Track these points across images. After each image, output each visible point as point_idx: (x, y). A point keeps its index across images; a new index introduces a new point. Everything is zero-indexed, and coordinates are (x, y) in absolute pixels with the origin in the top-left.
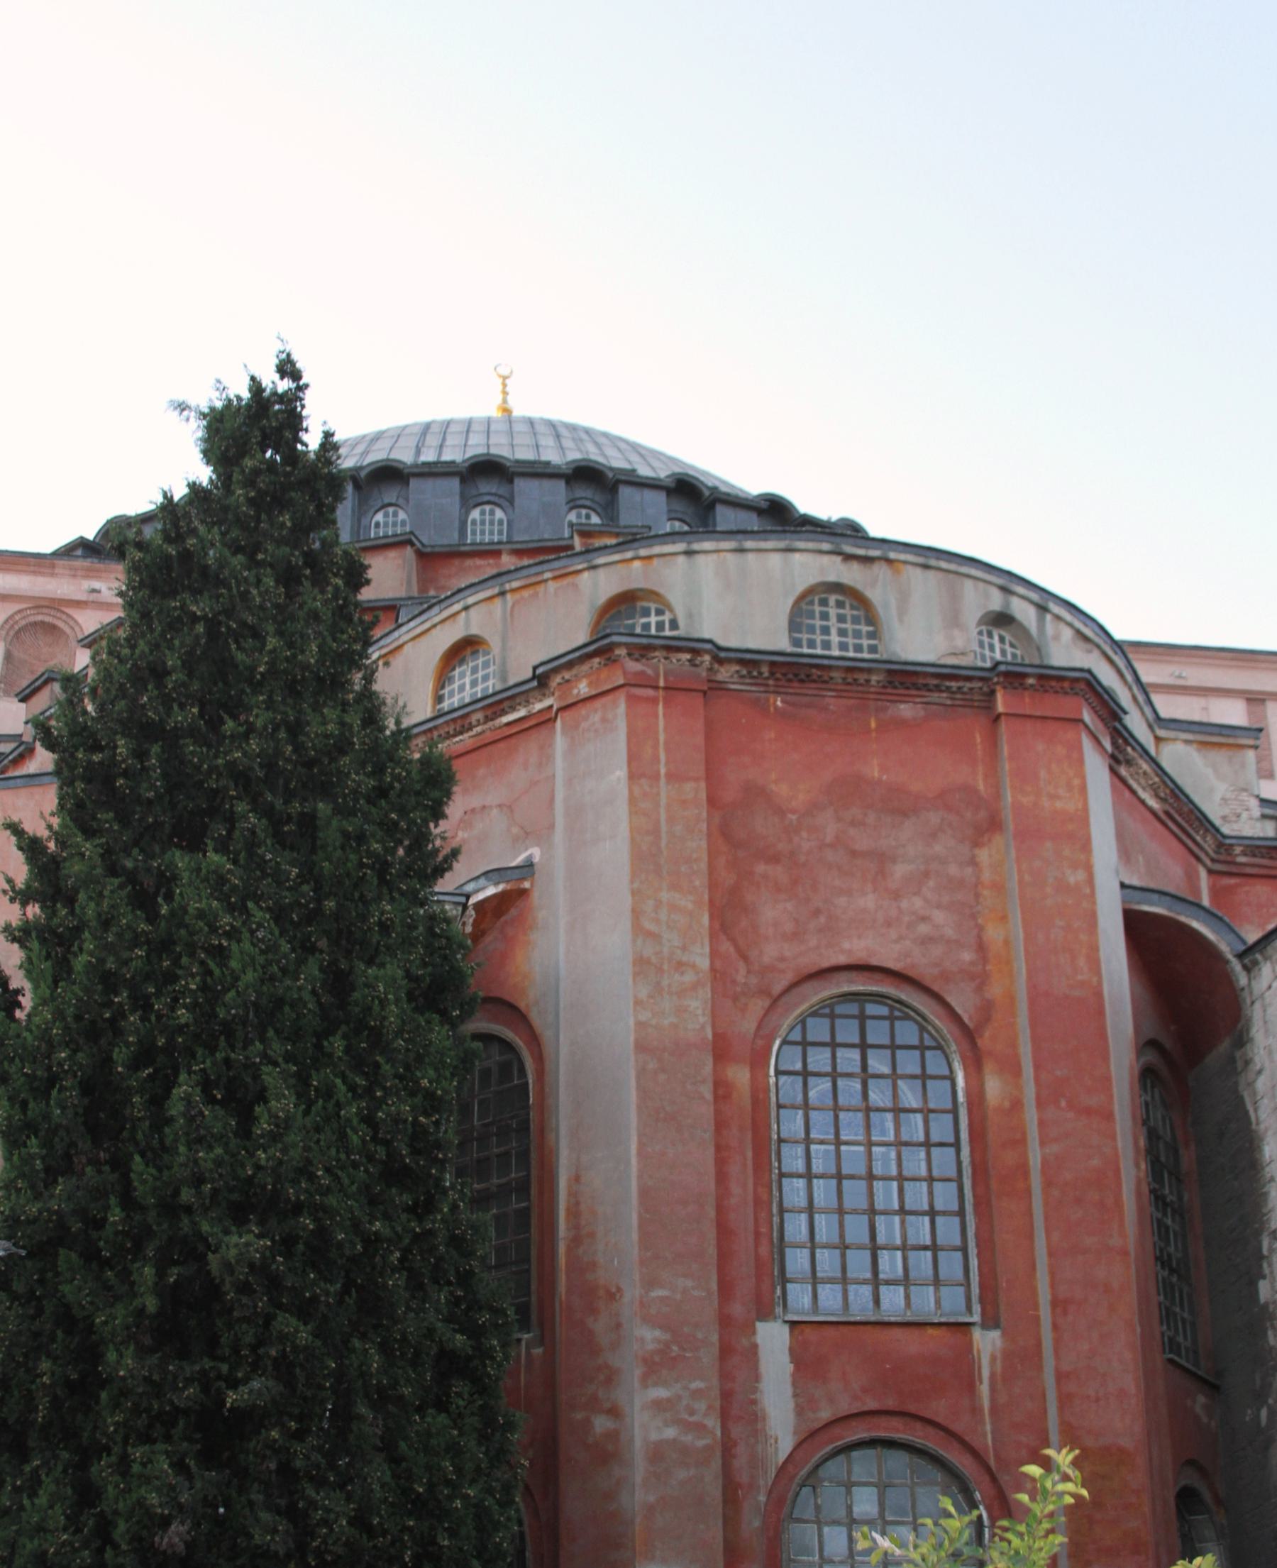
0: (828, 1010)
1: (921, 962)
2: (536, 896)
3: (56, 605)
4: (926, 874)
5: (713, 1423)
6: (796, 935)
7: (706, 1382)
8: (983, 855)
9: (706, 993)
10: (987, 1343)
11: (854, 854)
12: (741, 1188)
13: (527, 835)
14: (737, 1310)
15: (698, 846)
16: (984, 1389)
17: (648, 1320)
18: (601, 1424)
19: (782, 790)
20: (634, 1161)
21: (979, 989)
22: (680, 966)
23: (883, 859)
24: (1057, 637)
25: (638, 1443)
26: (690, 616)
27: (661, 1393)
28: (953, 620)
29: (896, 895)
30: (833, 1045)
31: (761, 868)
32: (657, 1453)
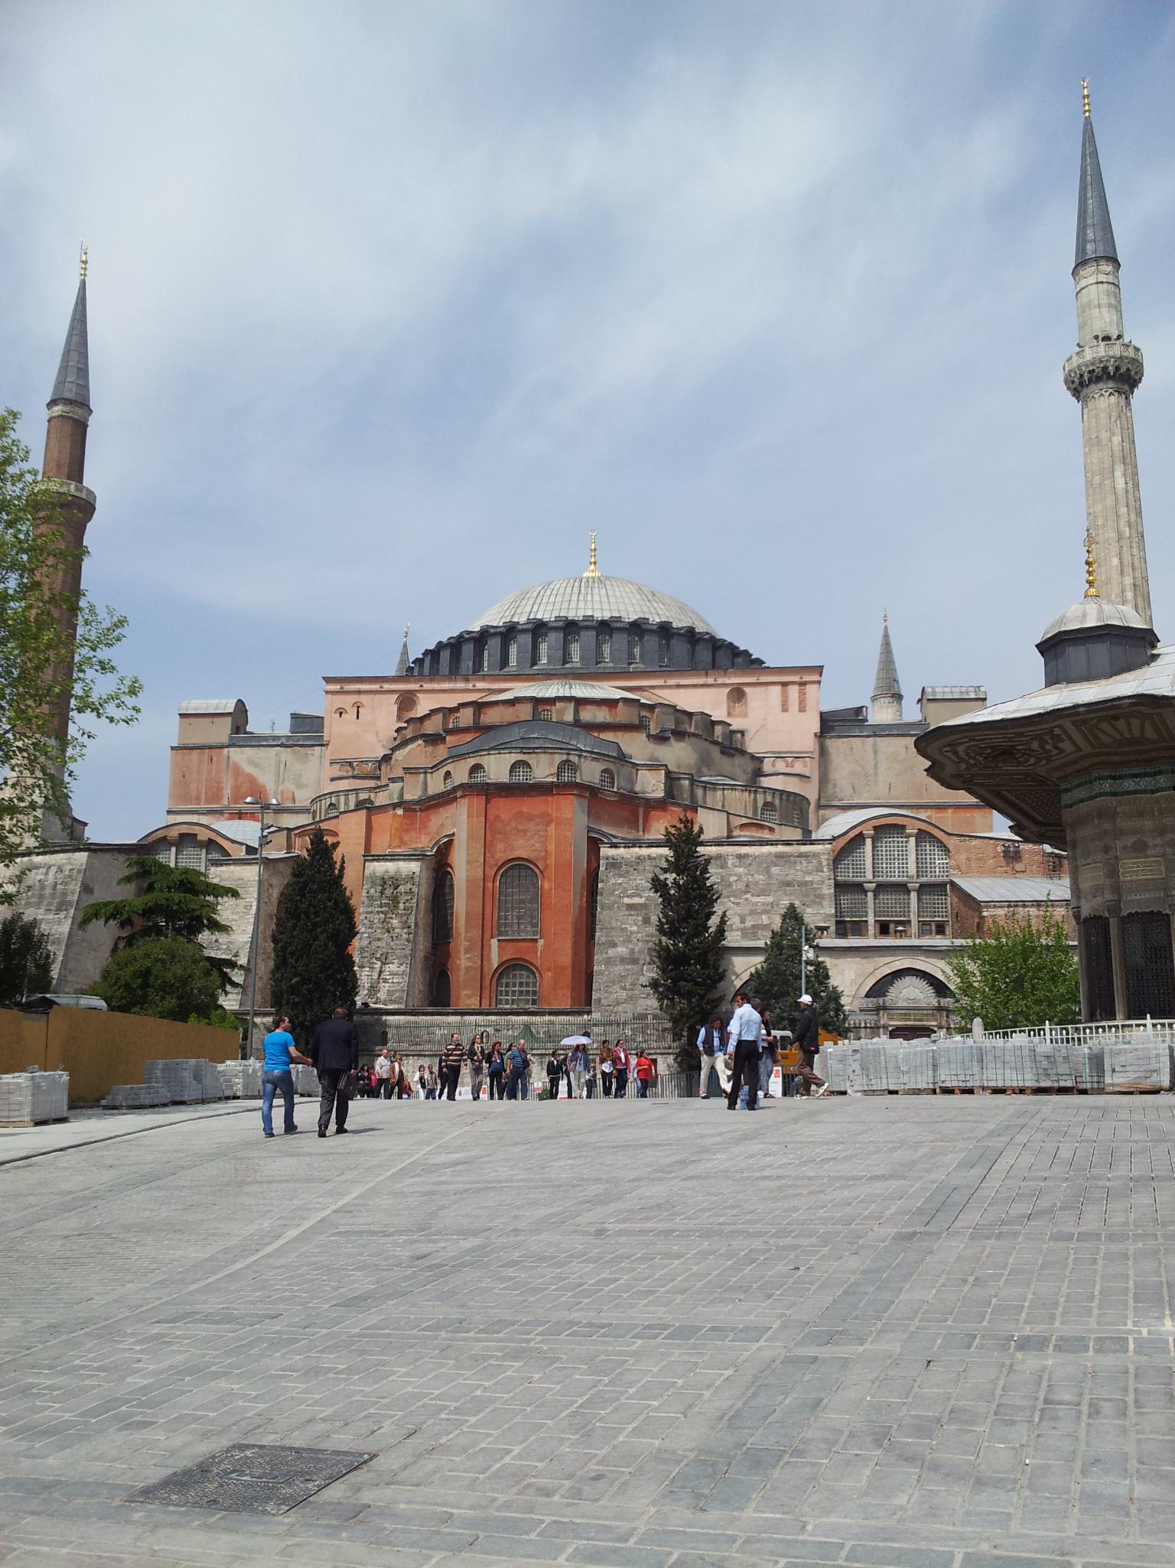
2: (455, 842)
3: (412, 692)
4: (535, 835)
5: (480, 962)
7: (478, 953)
10: (541, 942)
13: (454, 826)
14: (487, 936)
16: (539, 953)
17: (466, 940)
18: (458, 961)
21: (545, 862)
22: (477, 862)
23: (525, 832)
27: (468, 956)
28: (551, 765)
29: (528, 840)
31: (498, 836)
32: (467, 968)
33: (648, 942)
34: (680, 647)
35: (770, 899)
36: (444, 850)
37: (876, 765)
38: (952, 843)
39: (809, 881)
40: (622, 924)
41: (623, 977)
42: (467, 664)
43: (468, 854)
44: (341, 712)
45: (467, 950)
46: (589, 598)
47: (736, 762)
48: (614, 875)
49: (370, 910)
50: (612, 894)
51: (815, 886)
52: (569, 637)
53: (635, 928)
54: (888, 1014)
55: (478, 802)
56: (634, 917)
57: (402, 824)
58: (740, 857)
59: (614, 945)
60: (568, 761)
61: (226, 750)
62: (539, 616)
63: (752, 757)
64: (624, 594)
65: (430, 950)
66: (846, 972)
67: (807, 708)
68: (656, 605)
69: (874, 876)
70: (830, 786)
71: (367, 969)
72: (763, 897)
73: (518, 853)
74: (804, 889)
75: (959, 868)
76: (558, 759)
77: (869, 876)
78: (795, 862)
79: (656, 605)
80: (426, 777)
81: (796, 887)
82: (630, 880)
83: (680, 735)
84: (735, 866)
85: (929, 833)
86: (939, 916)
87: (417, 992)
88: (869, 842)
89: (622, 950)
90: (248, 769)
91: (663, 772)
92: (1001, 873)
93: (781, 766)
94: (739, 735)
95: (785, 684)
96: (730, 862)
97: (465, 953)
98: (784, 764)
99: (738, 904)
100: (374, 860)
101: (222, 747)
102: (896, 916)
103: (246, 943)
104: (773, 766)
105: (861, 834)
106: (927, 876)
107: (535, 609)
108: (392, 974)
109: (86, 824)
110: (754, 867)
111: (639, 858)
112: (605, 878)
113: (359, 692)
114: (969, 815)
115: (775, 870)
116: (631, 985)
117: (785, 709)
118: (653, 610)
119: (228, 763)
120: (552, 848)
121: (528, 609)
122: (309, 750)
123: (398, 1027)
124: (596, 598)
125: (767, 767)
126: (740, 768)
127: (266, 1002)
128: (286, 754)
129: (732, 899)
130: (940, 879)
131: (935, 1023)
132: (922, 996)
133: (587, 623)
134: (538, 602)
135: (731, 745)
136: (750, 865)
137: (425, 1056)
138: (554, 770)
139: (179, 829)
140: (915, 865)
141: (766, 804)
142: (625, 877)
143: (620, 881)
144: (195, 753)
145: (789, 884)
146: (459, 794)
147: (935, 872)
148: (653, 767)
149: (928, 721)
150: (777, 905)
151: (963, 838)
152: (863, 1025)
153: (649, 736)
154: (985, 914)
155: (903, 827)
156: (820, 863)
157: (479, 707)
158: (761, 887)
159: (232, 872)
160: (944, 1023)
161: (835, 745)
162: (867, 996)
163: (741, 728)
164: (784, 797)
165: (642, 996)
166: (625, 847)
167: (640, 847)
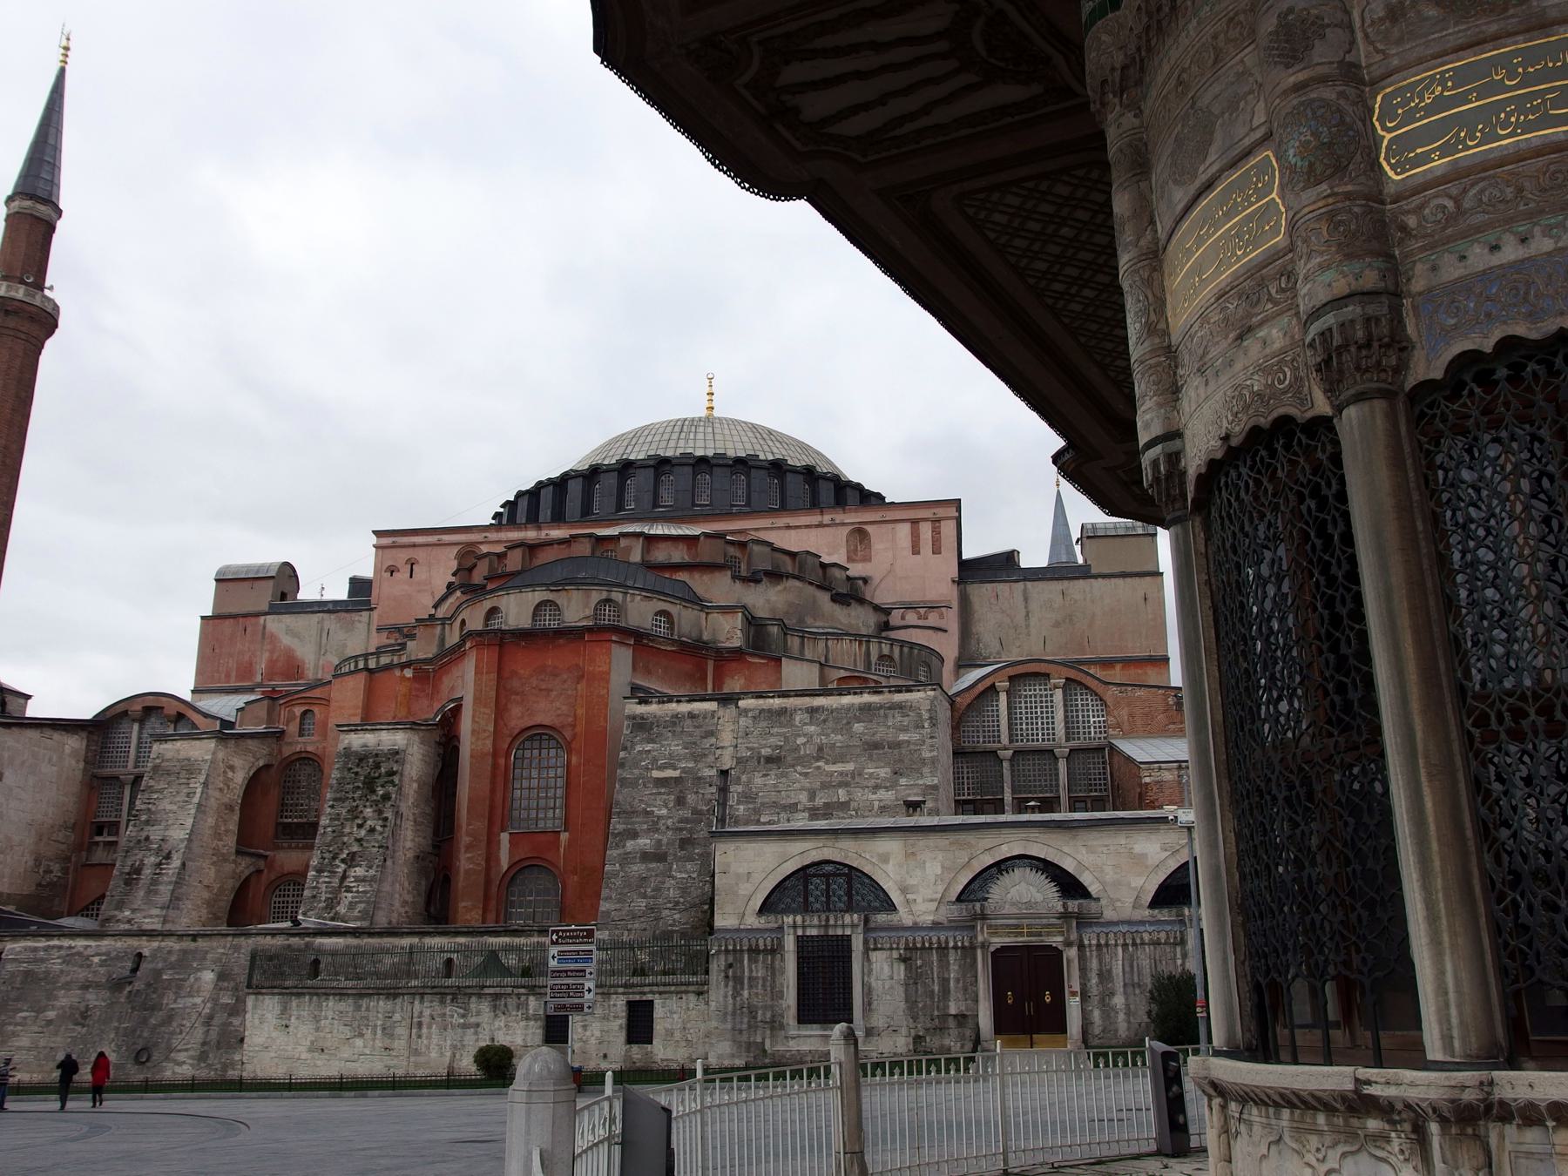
0: (531, 738)
1: (556, 722)
4: (561, 694)
5: (483, 863)
6: (522, 717)
8: (579, 686)
9: (492, 738)
10: (564, 836)
11: (541, 690)
12: (499, 795)
15: (493, 693)
16: (562, 850)
17: (468, 834)
19: (522, 672)
20: (467, 790)
22: (485, 731)
23: (549, 691)
24: (632, 601)
25: (462, 870)
26: (506, 615)
28: (586, 606)
29: (552, 702)
30: (532, 749)
31: (513, 697)
32: (467, 872)
33: (681, 829)
34: (795, 485)
35: (850, 767)
36: (450, 720)
37: (1027, 615)
38: (1111, 694)
39: (904, 741)
40: (649, 806)
41: (644, 879)
42: (545, 512)
43: (474, 721)
44: (392, 570)
45: (469, 848)
46: (692, 436)
47: (853, 614)
48: (641, 742)
49: (338, 795)
50: (636, 765)
51: (912, 747)
52: (663, 478)
53: (664, 812)
54: (990, 927)
55: (490, 655)
56: (664, 797)
57: (410, 689)
58: (812, 711)
59: (634, 835)
60: (608, 601)
61: (263, 618)
62: (632, 457)
63: (877, 608)
64: (735, 432)
65: (430, 849)
66: (928, 865)
67: (942, 549)
68: (771, 443)
69: (1011, 741)
70: (973, 642)
71: (325, 874)
72: (840, 765)
73: (539, 720)
74: (896, 752)
75: (1119, 726)
76: (597, 596)
77: (1005, 739)
78: (886, 716)
79: (771, 443)
80: (444, 629)
81: (886, 749)
82: (662, 746)
83: (776, 576)
84: (806, 724)
85: (1080, 683)
86: (1096, 791)
87: (397, 904)
88: (1003, 697)
89: (644, 842)
90: (286, 640)
91: (740, 614)
92: (1174, 732)
93: (911, 618)
94: (861, 582)
95: (915, 522)
96: (798, 718)
97: (466, 852)
98: (915, 616)
99: (806, 775)
100: (351, 731)
101: (257, 615)
102: (1041, 792)
103: (182, 840)
104: (903, 618)
105: (993, 686)
106: (1079, 739)
107: (630, 448)
108: (358, 880)
109: (28, 697)
110: (830, 724)
111: (676, 716)
112: (629, 744)
113: (414, 546)
114: (1140, 671)
115: (858, 727)
116: (653, 890)
117: (916, 550)
118: (766, 447)
119: (264, 634)
120: (581, 711)
121: (621, 451)
122: (355, 616)
123: (334, 953)
124: (700, 436)
125: (895, 619)
126: (859, 619)
127: (215, 918)
128: (330, 621)
129: (799, 768)
130: (1095, 743)
131: (1060, 939)
132: (1039, 897)
133: (684, 460)
134: (633, 443)
135: (851, 593)
136: (825, 721)
137: (348, 995)
138: (589, 612)
139: (143, 701)
140: (1063, 724)
141: (881, 657)
142: (655, 743)
143: (649, 747)
144: (228, 622)
145: (876, 746)
146: (468, 645)
147: (1090, 733)
148: (727, 610)
149: (1089, 563)
150: (860, 775)
151: (1123, 688)
152: (951, 944)
153: (734, 578)
154: (1147, 780)
155: (1047, 676)
156: (920, 715)
157: (532, 548)
158: (838, 750)
159: (178, 751)
160: (1074, 936)
161: (981, 593)
162: (959, 899)
163: (864, 575)
164: (906, 650)
165: (669, 905)
166: (659, 702)
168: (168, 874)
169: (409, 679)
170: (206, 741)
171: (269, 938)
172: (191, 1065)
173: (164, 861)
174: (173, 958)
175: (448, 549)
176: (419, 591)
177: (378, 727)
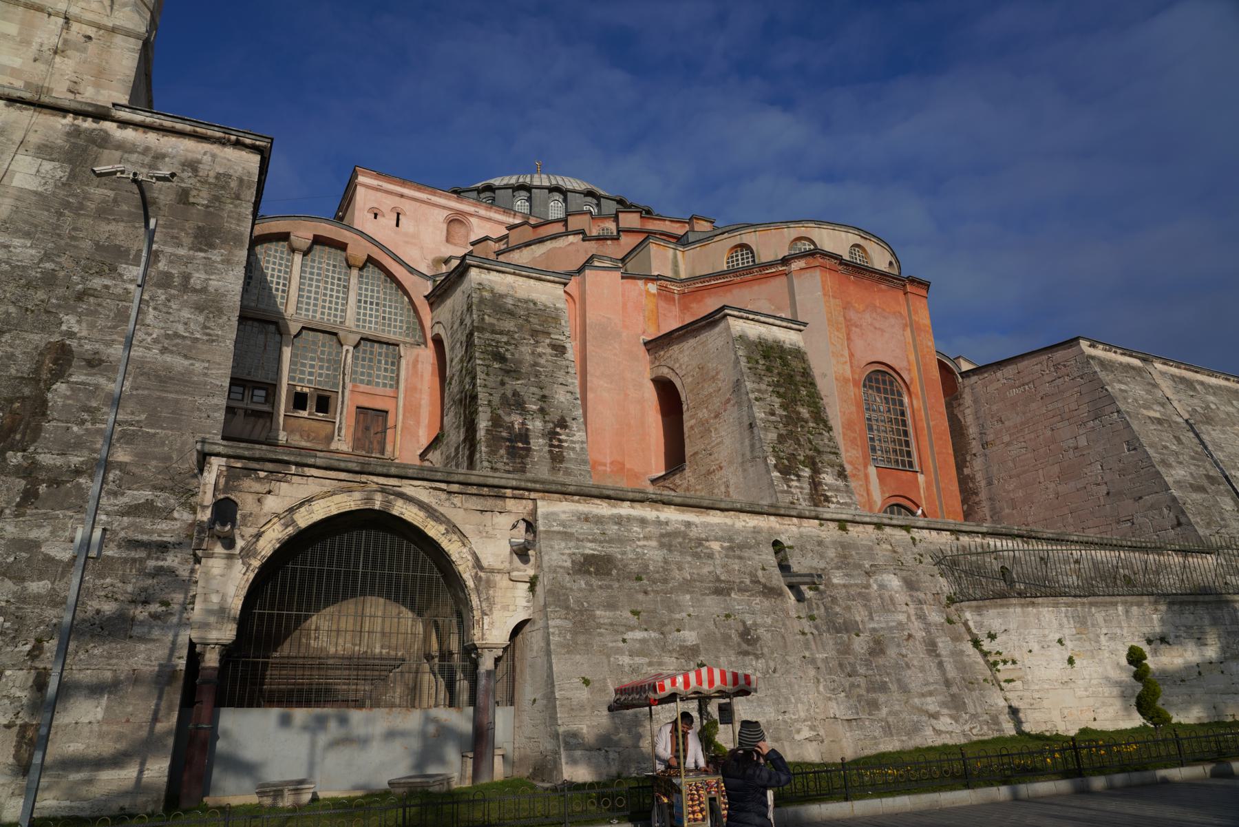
5: (865, 494)
16: (922, 491)
22: (842, 355)
23: (883, 331)
100: (741, 318)
113: (402, 196)
167: (1115, 352)
168: (574, 449)
169: (654, 295)
170: (550, 285)
171: (934, 533)
172: (951, 716)
173: (558, 430)
174: (831, 553)
175: (437, 211)
176: (407, 242)
177: (771, 320)
